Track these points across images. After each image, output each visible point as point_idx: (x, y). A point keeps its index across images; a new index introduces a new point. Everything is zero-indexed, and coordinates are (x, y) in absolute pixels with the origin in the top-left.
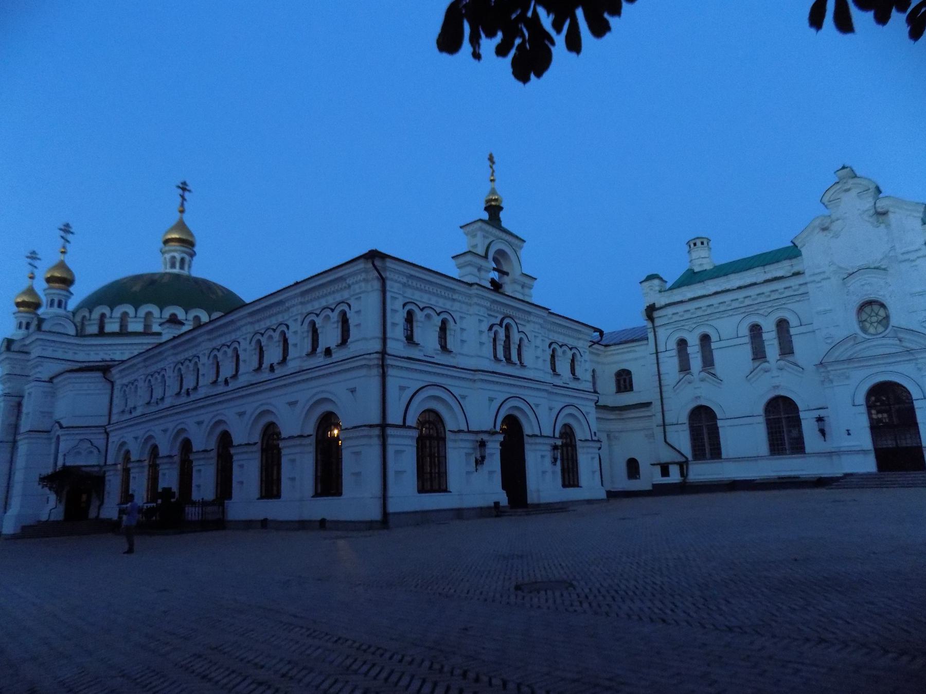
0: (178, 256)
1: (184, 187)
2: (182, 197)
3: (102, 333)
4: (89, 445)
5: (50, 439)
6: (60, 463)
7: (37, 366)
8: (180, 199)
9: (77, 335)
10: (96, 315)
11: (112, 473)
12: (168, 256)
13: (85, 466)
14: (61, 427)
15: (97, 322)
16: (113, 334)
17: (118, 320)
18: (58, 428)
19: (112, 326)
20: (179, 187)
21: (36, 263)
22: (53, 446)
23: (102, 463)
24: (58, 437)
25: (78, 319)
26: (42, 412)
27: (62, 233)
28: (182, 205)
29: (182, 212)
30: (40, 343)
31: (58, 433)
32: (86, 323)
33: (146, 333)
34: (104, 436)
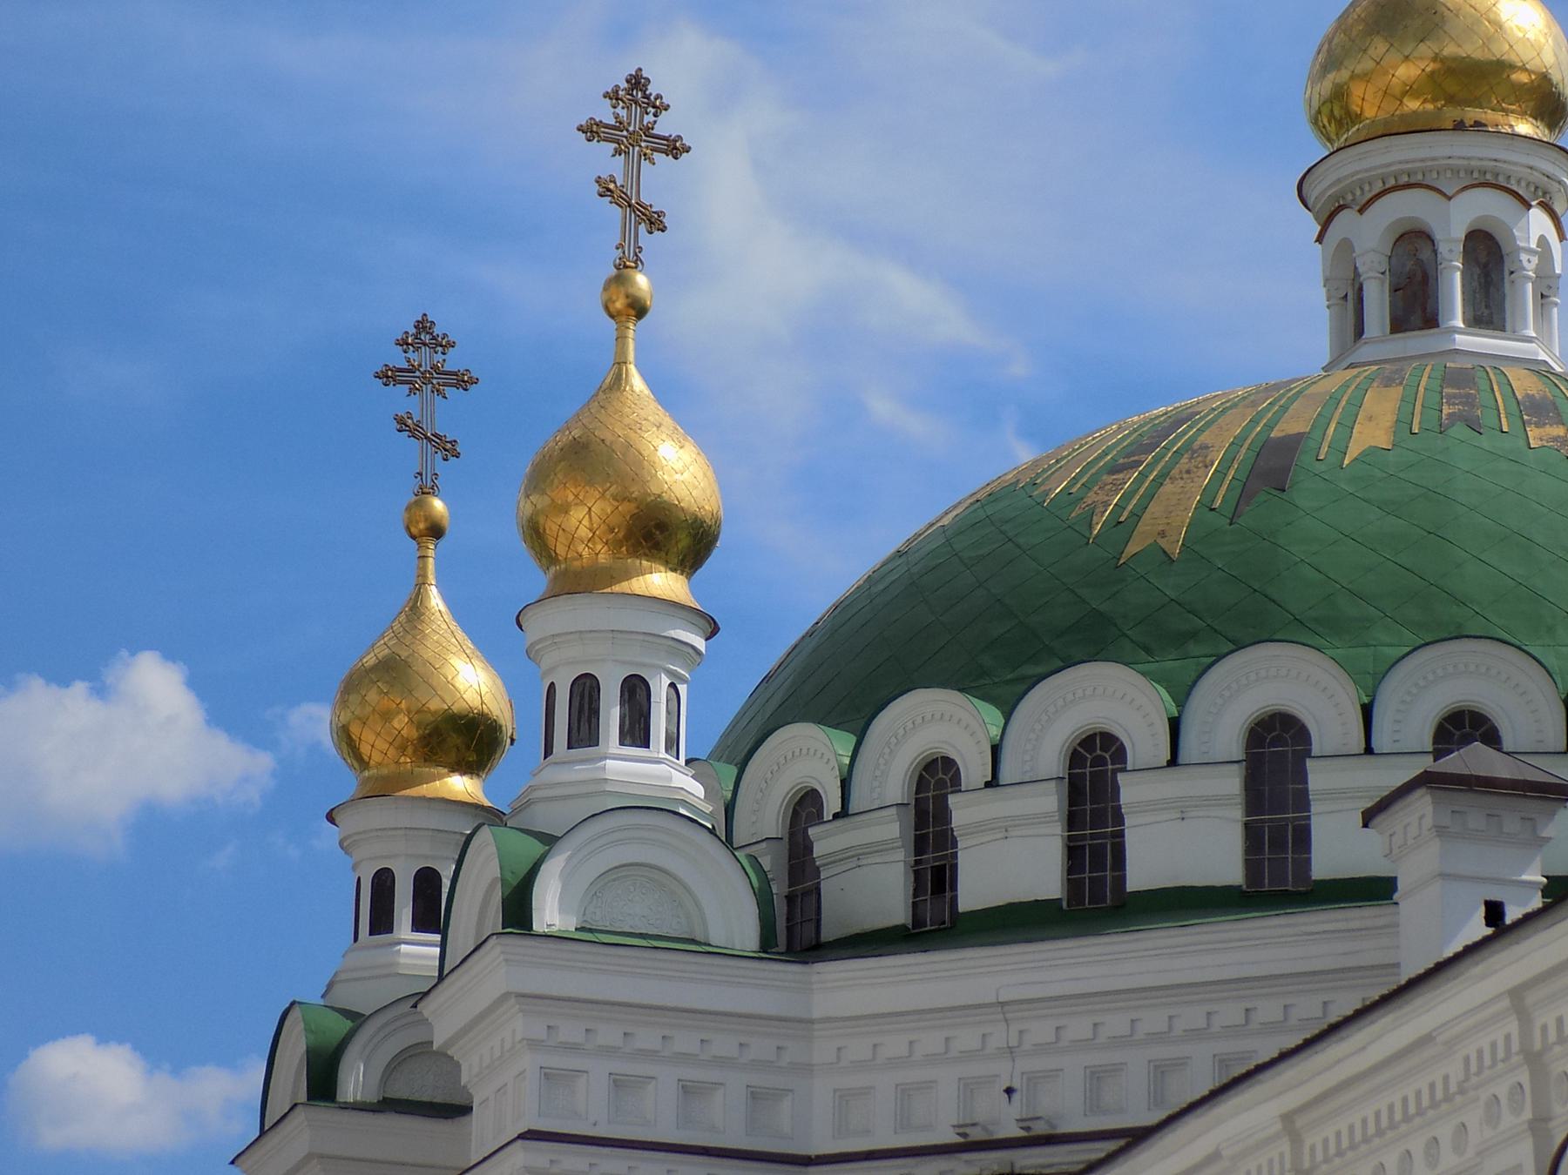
0: (1452, 222)
3: (937, 917)
9: (767, 943)
12: (1369, 235)
16: (1016, 922)
17: (1049, 802)
19: (1008, 855)
21: (449, 413)
25: (764, 816)
27: (604, 160)
32: (826, 841)
33: (1277, 875)
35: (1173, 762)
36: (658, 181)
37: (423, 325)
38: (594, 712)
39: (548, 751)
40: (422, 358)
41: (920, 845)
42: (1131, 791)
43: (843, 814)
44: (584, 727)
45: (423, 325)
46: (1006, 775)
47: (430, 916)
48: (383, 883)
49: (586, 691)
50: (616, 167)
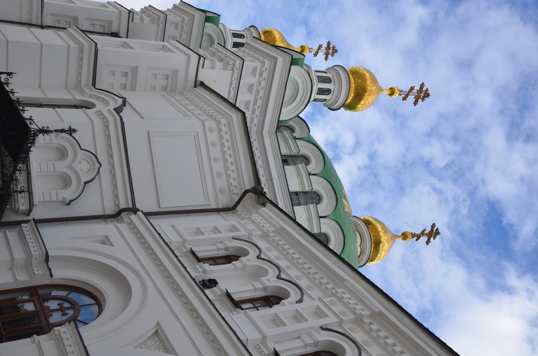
1: (433, 233)
2: (423, 233)
4: (85, 178)
5: (78, 87)
6: (37, 117)
7: (221, 60)
8: (418, 232)
10: (304, 149)
11: (19, 254)
13: (29, 174)
14: (118, 110)
15: (294, 152)
17: (307, 189)
18: (113, 105)
20: (433, 225)
22: (64, 96)
23: (38, 213)
24: (87, 106)
26: (135, 70)
27: (417, 88)
28: (413, 235)
29: (405, 236)
30: (267, 64)
31: (100, 106)
34: (110, 210)
35: (321, 217)
36: (411, 99)
37: (336, 51)
38: (324, 82)
39: (316, 71)
40: (331, 51)
41: (291, 156)
42: (311, 206)
43: (295, 138)
44: (321, 80)
45: (336, 51)
46: (311, 177)
47: (236, 45)
48: (241, 36)
49: (328, 80)
50: (415, 91)
